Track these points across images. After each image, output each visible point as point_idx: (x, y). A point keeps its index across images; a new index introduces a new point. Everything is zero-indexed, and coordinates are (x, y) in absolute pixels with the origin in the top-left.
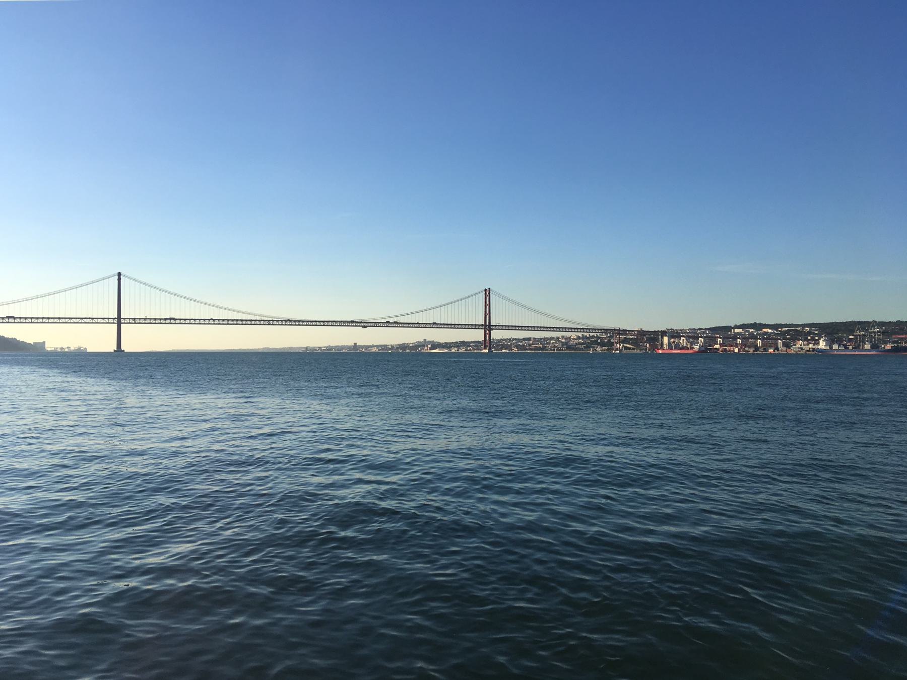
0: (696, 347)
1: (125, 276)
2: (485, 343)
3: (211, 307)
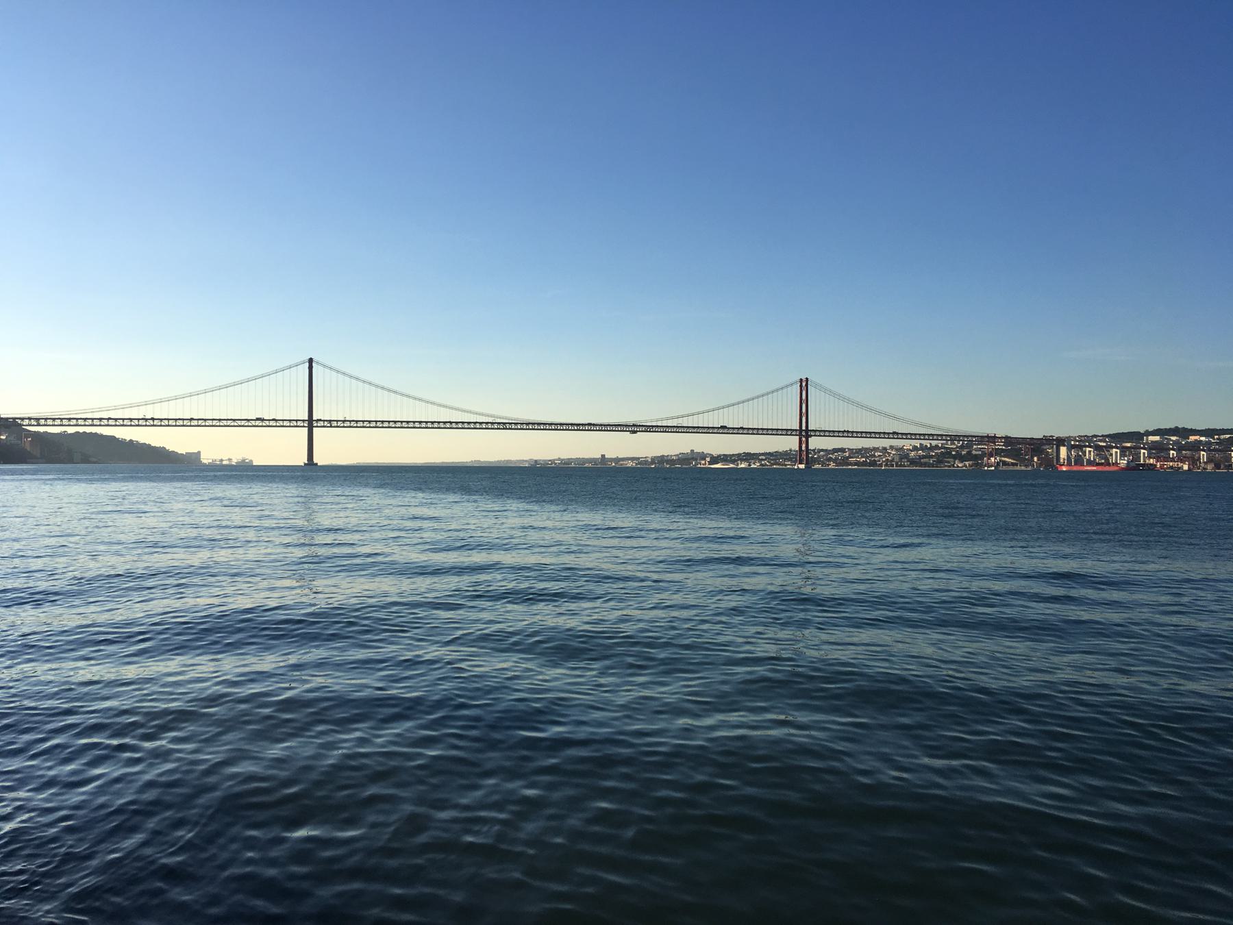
2: (801, 455)
3: (430, 405)
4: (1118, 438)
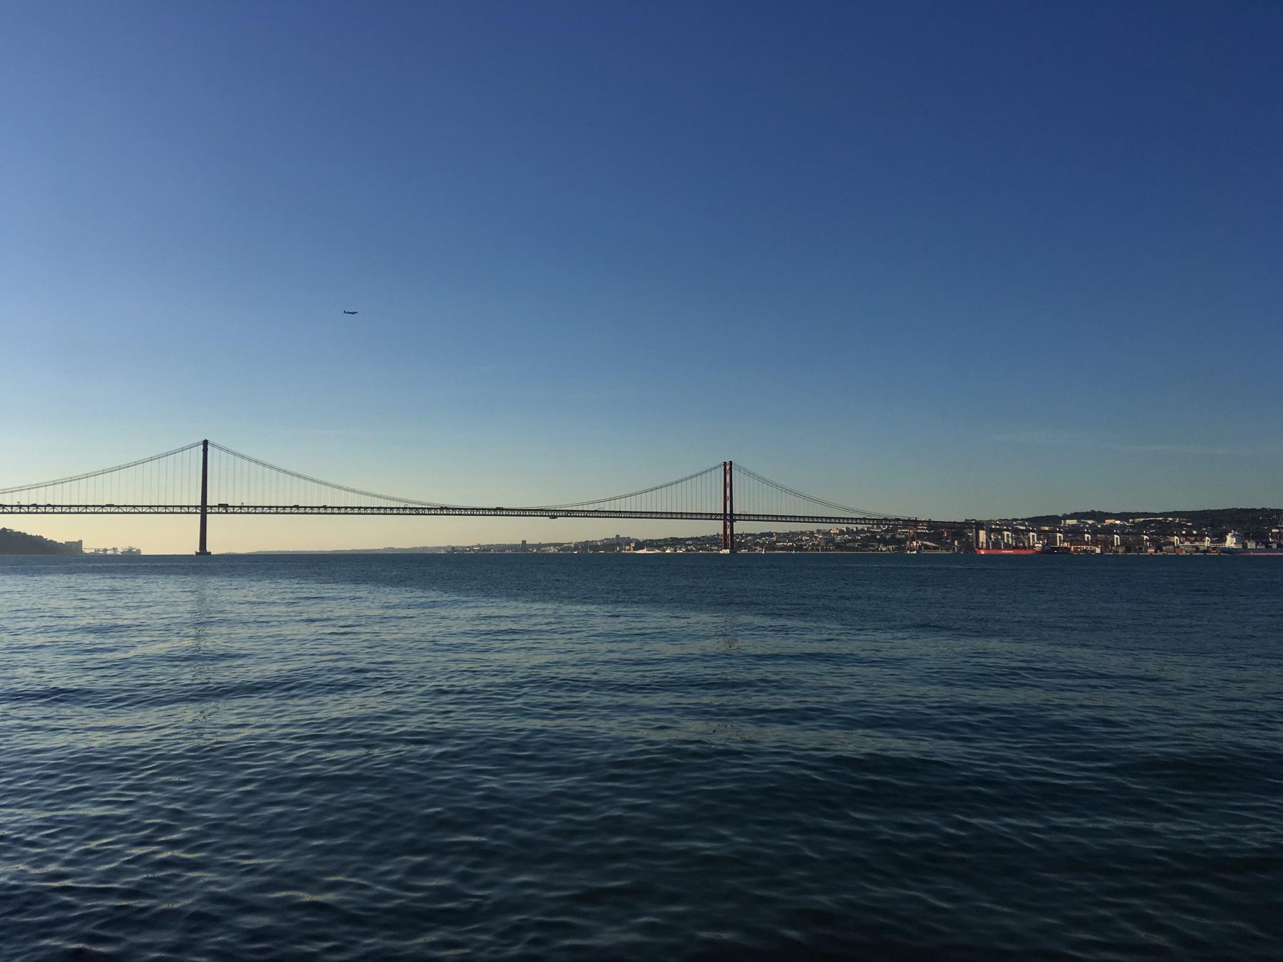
1: (213, 445)
2: (725, 540)
4: (1036, 522)
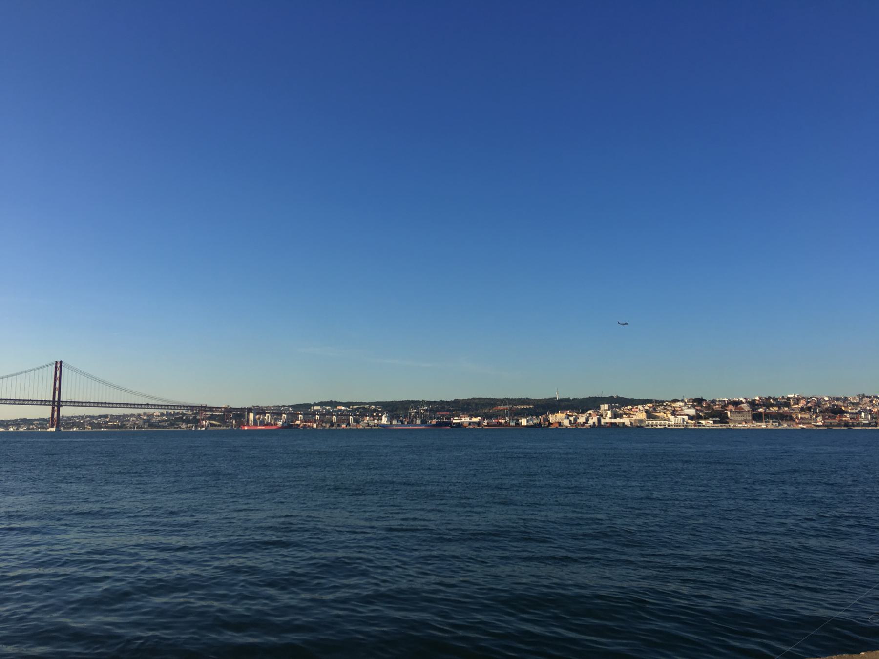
0: (279, 423)
2: (52, 420)
